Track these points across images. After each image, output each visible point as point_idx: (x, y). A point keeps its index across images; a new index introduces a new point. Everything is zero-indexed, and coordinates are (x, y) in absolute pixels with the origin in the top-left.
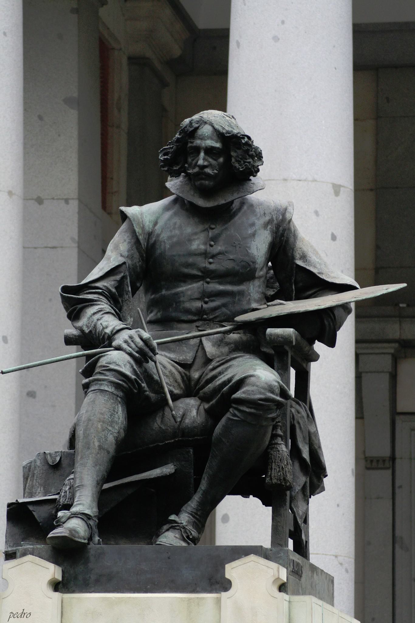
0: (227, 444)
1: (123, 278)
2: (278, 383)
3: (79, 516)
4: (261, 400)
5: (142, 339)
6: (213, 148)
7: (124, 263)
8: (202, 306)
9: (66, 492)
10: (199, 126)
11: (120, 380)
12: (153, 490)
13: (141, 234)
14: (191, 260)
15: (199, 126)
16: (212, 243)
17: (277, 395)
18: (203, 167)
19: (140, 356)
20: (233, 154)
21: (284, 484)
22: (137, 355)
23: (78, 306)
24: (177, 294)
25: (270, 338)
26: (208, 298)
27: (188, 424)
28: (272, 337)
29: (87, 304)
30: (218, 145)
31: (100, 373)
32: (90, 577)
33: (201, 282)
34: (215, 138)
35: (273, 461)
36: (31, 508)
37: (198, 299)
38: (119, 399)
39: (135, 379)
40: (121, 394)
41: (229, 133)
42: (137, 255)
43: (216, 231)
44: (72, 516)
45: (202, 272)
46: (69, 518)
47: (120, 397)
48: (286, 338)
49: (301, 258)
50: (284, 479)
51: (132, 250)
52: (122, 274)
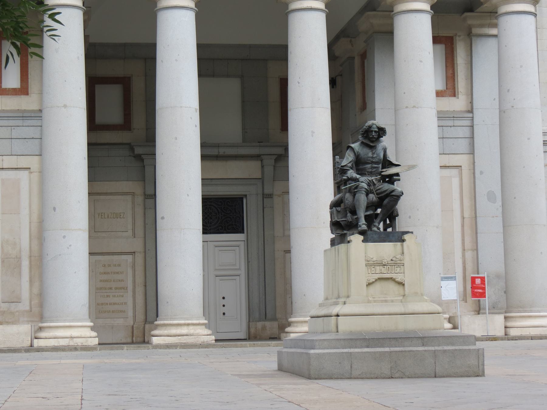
1: (353, 163)
5: (368, 180)
9: (349, 218)
14: (369, 159)
18: (373, 136)
20: (380, 132)
24: (365, 167)
30: (377, 130)
34: (377, 128)
36: (340, 222)
37: (371, 169)
40: (366, 194)
42: (355, 158)
43: (374, 151)
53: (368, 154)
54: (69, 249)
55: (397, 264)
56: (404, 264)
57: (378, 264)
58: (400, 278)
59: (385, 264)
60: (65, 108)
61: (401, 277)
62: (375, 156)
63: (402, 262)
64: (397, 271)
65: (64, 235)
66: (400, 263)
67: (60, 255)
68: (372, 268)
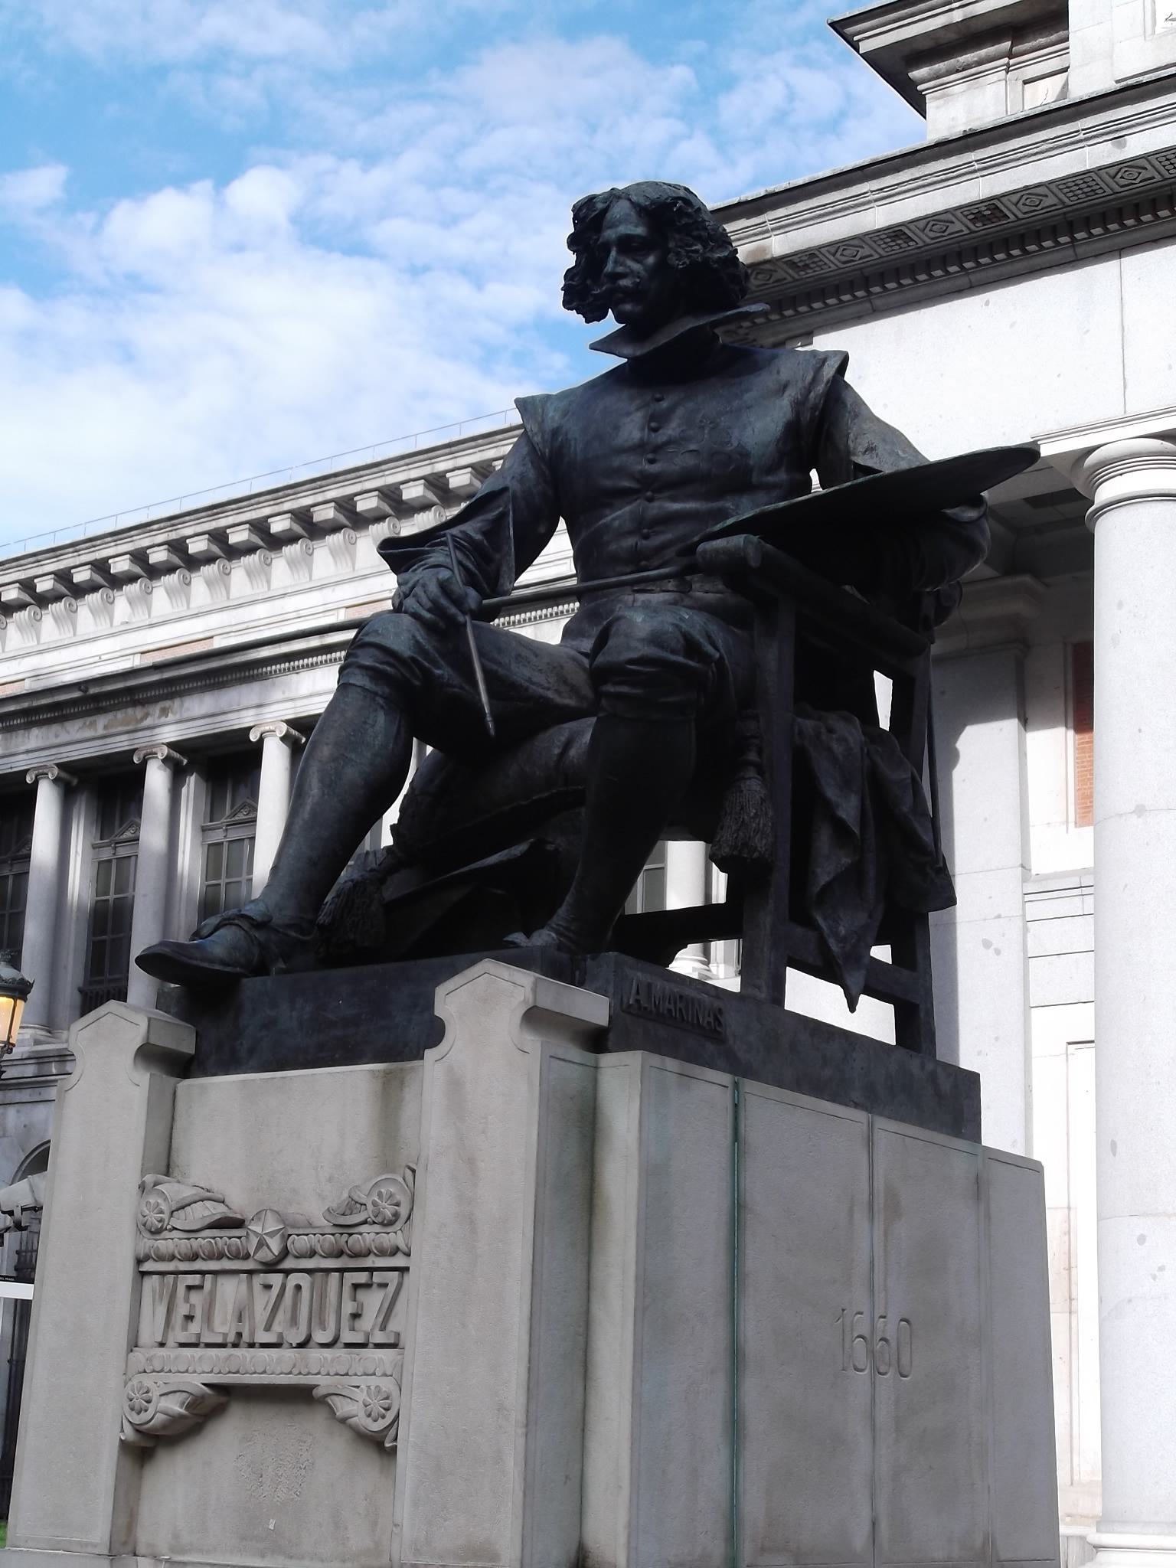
1: (503, 516)
2: (677, 626)
3: (236, 922)
4: (632, 661)
7: (505, 490)
8: (637, 544)
10: (608, 207)
11: (382, 663)
12: (499, 892)
13: (536, 434)
14: (616, 462)
15: (608, 207)
16: (653, 425)
17: (673, 652)
19: (433, 616)
21: (745, 856)
22: (427, 615)
26: (649, 528)
27: (573, 757)
30: (640, 231)
33: (638, 501)
35: (728, 812)
37: (631, 533)
38: (381, 701)
39: (413, 659)
42: (532, 474)
44: (224, 922)
45: (638, 481)
46: (217, 928)
47: (381, 696)
49: (866, 451)
50: (745, 845)
51: (524, 465)
52: (501, 509)
53: (617, 428)
54: (1157, 1280)
55: (356, 1255)
56: (408, 1255)
57: (220, 1256)
58: (361, 1396)
59: (264, 1255)
60: (1139, 817)
61: (373, 1381)
62: (671, 430)
63: (393, 1238)
64: (358, 1323)
65: (1142, 1232)
66: (382, 1253)
67: (1130, 1301)
68: (181, 1291)
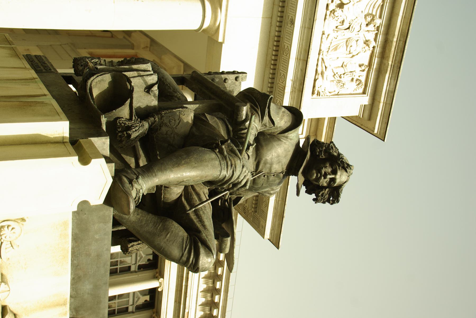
0: (166, 239)
3: (138, 195)
6: (335, 182)
7: (274, 126)
10: (347, 173)
20: (327, 190)
23: (259, 110)
25: (226, 240)
28: (226, 242)
29: (260, 118)
31: (232, 165)
32: (85, 214)
36: (128, 102)
41: (341, 192)
44: (138, 191)
48: (224, 250)
